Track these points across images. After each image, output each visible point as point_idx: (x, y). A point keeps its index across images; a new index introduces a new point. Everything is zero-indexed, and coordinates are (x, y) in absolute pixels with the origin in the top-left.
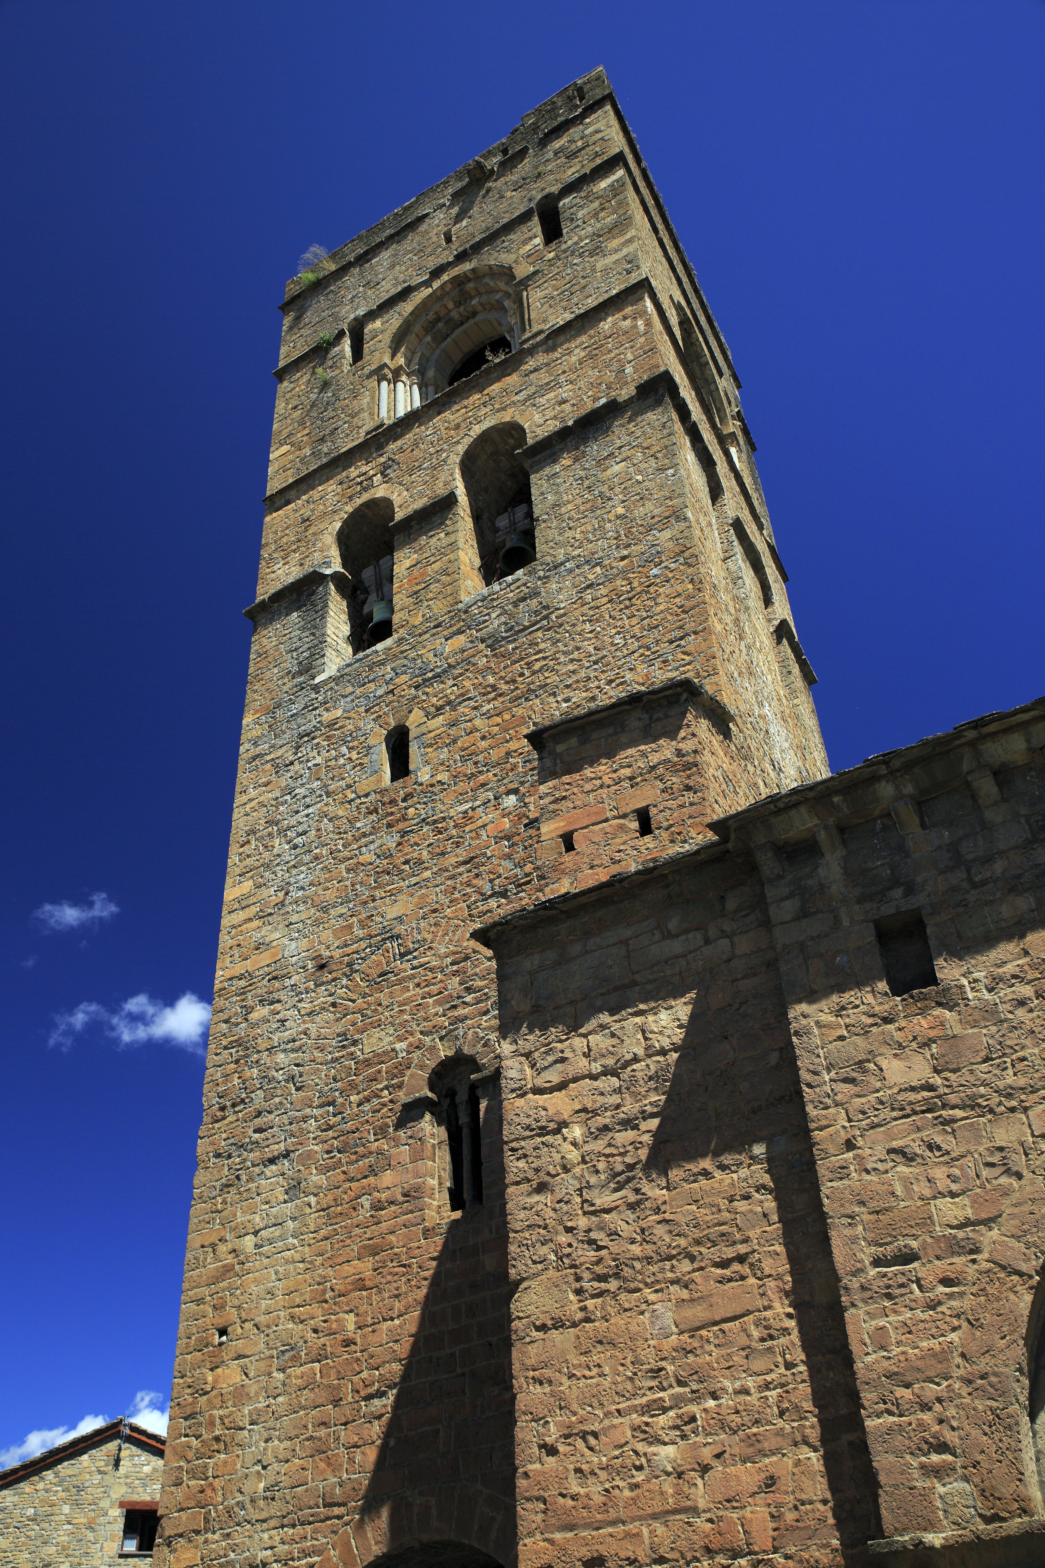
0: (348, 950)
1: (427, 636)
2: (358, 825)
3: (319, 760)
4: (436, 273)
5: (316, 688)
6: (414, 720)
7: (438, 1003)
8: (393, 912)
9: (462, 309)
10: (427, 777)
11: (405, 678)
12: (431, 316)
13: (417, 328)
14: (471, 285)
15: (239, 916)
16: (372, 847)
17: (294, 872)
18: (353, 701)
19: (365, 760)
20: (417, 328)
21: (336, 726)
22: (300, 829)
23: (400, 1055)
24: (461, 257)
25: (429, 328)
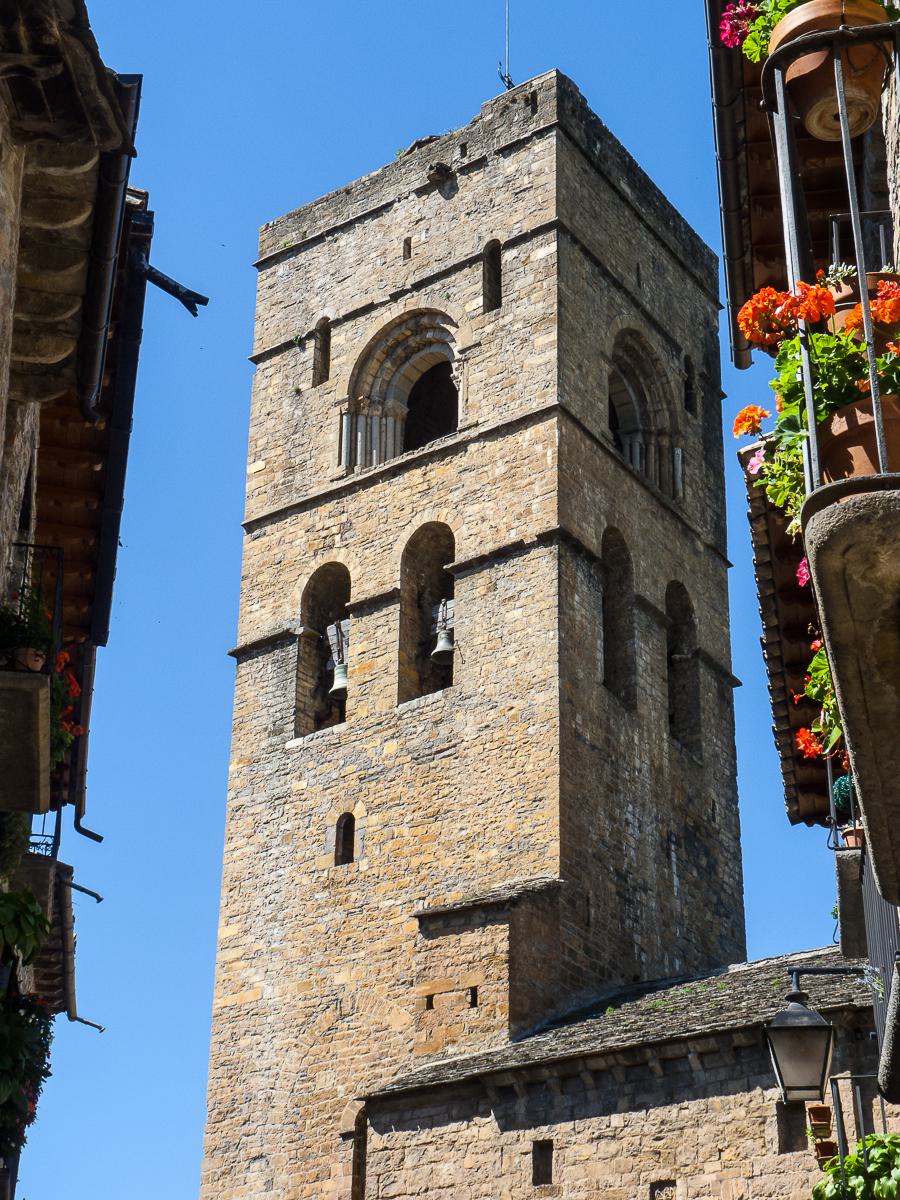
0: (309, 1003)
1: (370, 732)
2: (317, 896)
3: (288, 826)
4: (395, 297)
5: (286, 752)
6: (359, 811)
7: (364, 1060)
8: (339, 979)
9: (418, 339)
10: (366, 868)
11: (353, 768)
12: (391, 342)
13: (378, 354)
14: (425, 320)
15: (231, 954)
16: (326, 919)
17: (271, 925)
18: (315, 776)
19: (322, 837)
20: (378, 354)
21: (303, 797)
22: (275, 887)
23: (340, 1095)
24: (418, 286)
25: (389, 354)
